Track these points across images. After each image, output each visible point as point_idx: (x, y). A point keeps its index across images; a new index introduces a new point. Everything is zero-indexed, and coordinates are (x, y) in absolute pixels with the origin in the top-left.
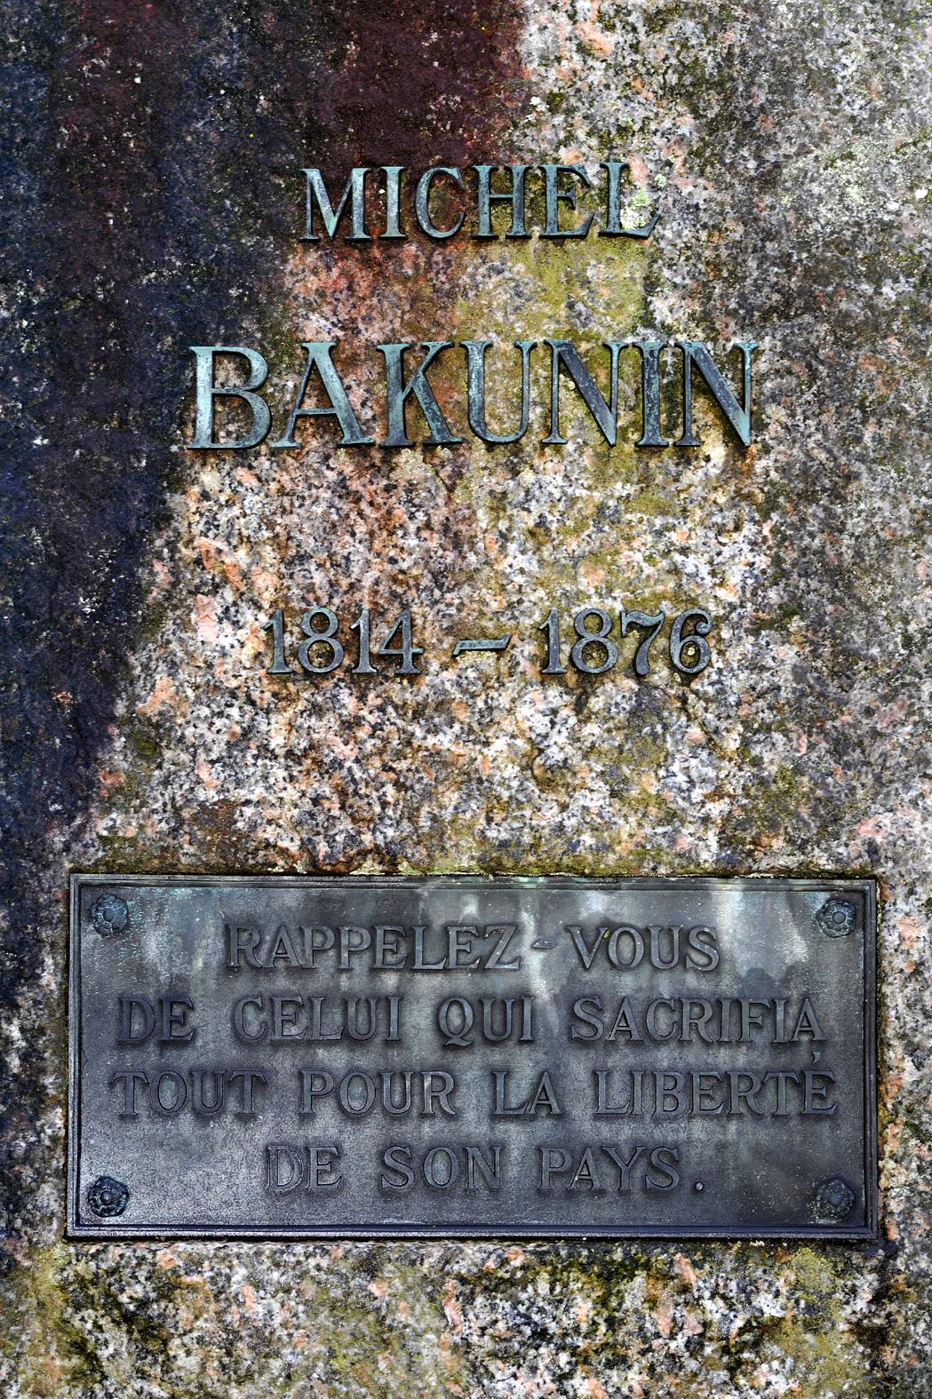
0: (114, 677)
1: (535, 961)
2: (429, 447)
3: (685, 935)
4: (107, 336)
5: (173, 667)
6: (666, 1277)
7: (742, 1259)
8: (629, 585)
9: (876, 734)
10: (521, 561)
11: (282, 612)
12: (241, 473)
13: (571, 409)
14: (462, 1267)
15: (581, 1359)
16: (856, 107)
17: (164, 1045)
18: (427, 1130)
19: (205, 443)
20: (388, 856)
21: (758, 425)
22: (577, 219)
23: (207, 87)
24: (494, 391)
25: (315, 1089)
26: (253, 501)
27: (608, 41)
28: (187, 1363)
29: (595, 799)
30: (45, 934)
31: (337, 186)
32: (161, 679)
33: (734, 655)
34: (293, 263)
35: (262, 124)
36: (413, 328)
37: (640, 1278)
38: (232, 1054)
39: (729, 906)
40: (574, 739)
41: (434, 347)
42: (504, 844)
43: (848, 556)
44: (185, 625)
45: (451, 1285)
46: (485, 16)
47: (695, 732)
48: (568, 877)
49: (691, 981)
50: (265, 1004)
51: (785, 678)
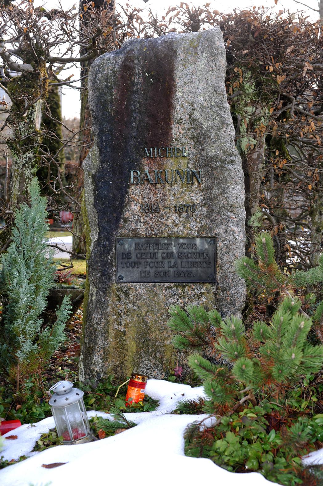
0: (121, 212)
1: (174, 248)
2: (160, 183)
3: (193, 245)
4: (119, 169)
5: (129, 211)
6: (190, 287)
7: (200, 285)
8: (186, 201)
9: (216, 219)
10: (172, 198)
11: (142, 204)
12: (137, 187)
13: (178, 179)
14: (165, 286)
15: (180, 297)
16: (214, 140)
17: (128, 259)
18: (161, 269)
19: (132, 183)
20: (156, 235)
21: (202, 181)
22: (179, 154)
23: (132, 137)
24: (168, 176)
25: (147, 264)
26: (138, 190)
27: (183, 132)
28: (131, 298)
29: (181, 228)
30: (113, 245)
31: (149, 150)
32: (127, 213)
33: (199, 210)
34: (143, 160)
35: (139, 142)
36: (158, 168)
37: (187, 287)
38: (136, 260)
39: (198, 241)
40: (179, 220)
41: (161, 171)
42: (170, 234)
43: (213, 197)
44: (130, 206)
45: (164, 288)
46: (167, 129)
47: (194, 219)
48: (178, 238)
49: (193, 250)
50: (141, 254)
51: (205, 213)
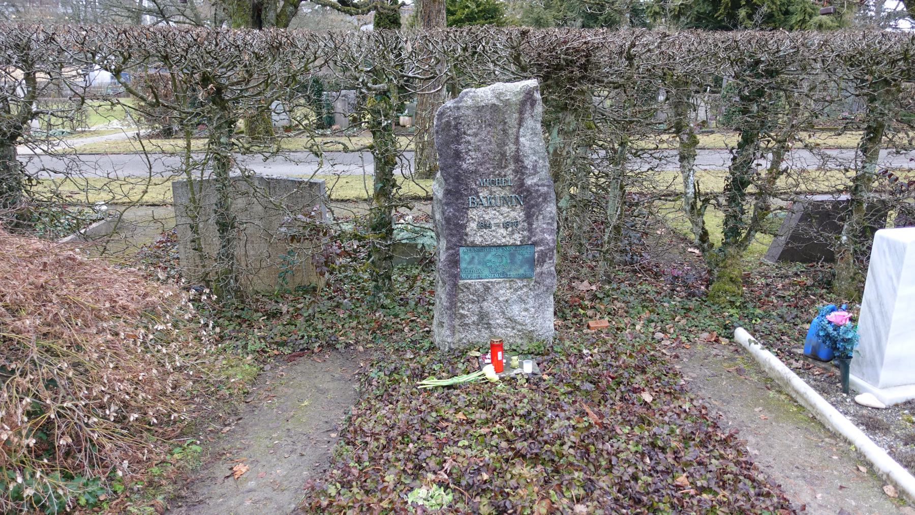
29: (508, 239)
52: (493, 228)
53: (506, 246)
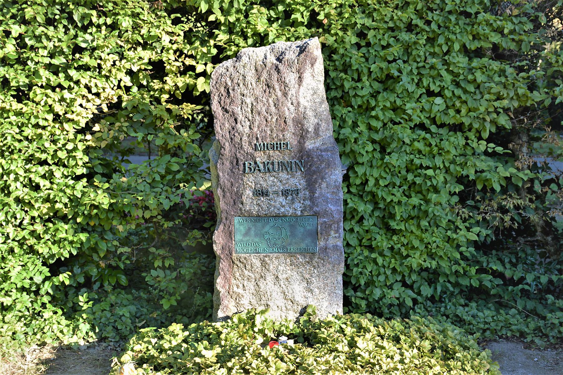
29: (288, 209)
52: (271, 196)
53: (285, 216)
